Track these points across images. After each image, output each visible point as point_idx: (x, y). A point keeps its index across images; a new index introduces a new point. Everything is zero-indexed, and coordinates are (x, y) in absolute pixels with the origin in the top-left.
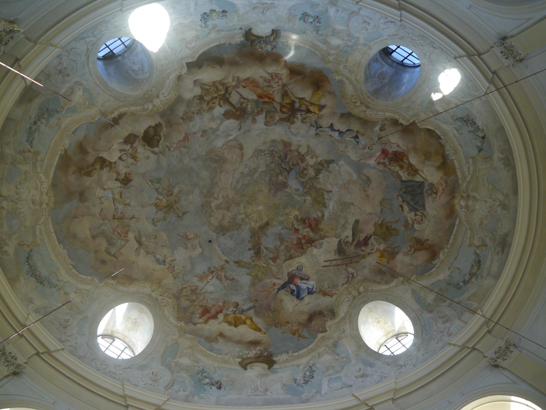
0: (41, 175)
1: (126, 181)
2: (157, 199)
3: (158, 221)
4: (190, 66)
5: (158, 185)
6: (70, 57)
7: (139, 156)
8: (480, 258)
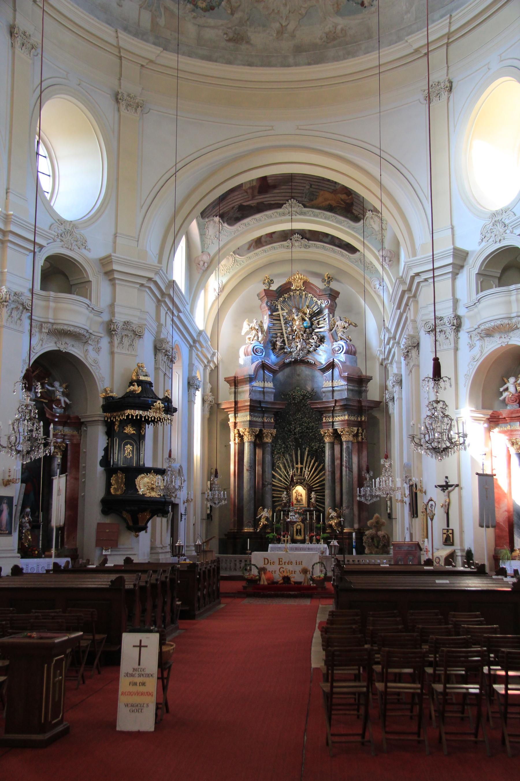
8: (216, 9)
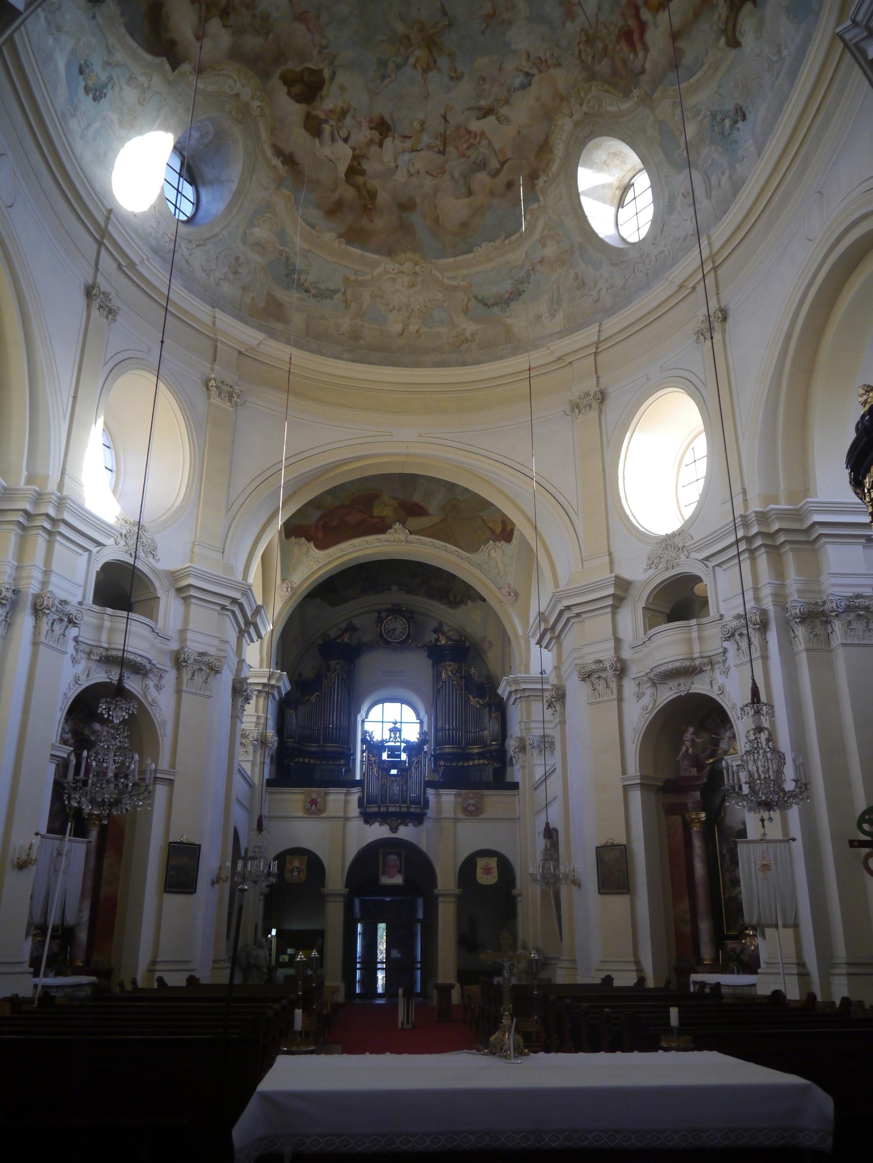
0: (375, 273)
1: (383, 127)
2: (414, 67)
3: (455, 69)
4: (175, 65)
5: (391, 66)
6: (214, 267)
7: (341, 104)
